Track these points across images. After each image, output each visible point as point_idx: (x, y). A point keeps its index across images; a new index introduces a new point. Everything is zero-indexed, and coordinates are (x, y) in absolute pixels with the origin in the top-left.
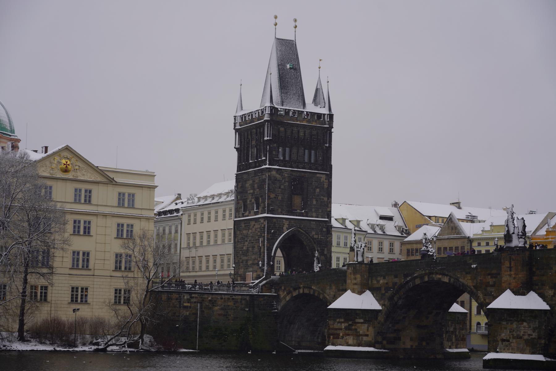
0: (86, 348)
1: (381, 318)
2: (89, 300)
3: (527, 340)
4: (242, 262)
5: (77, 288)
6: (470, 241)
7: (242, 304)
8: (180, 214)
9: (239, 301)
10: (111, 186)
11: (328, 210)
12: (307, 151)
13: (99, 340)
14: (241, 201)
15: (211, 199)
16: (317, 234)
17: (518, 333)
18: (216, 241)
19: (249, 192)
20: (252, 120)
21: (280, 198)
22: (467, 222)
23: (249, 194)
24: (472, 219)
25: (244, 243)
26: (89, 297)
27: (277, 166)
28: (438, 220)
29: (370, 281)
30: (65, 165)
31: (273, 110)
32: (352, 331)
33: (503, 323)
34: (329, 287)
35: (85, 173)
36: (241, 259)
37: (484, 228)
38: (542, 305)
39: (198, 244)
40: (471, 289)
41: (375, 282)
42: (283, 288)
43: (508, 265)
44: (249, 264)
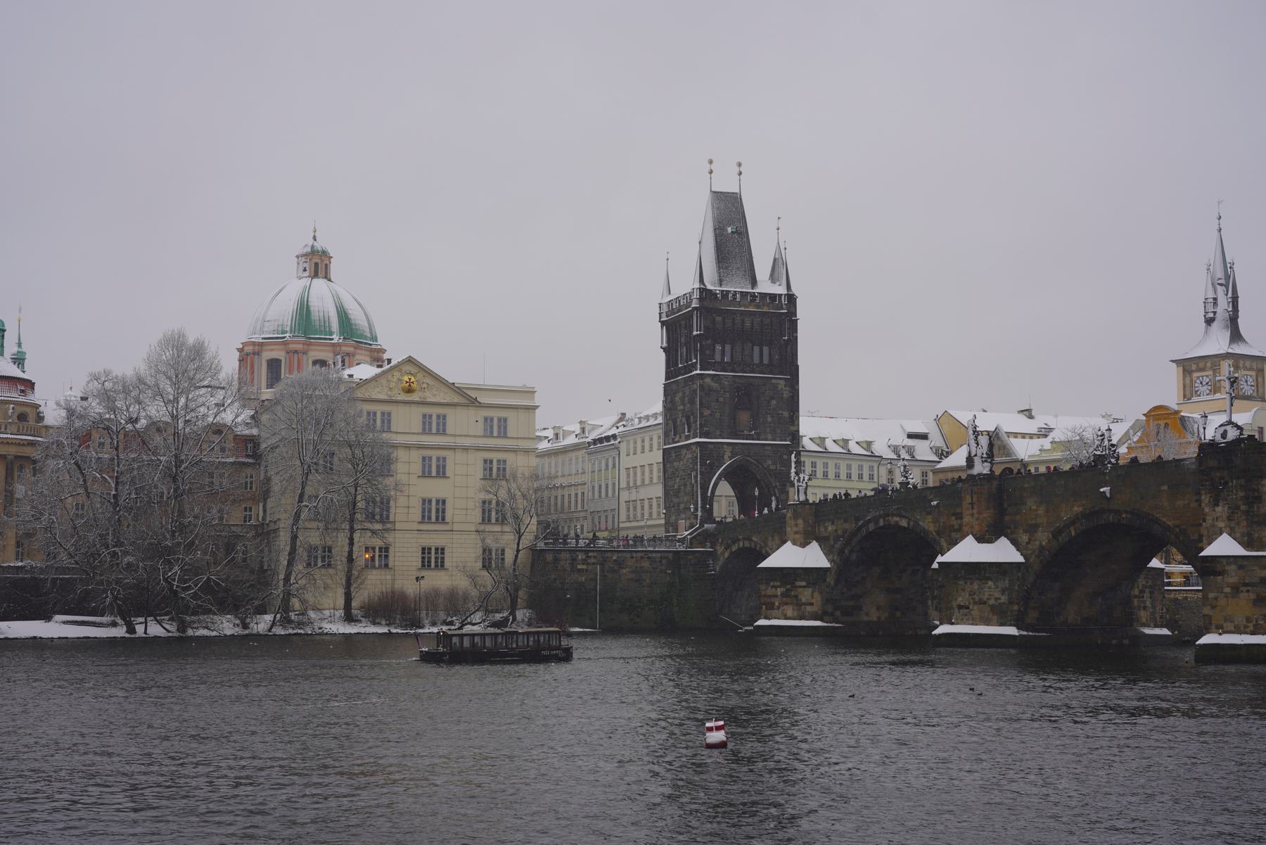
1: (830, 580)
2: (447, 564)
3: (993, 605)
4: (674, 506)
5: (430, 549)
7: (662, 565)
8: (617, 442)
9: (657, 560)
10: (473, 408)
12: (756, 349)
17: (982, 596)
19: (679, 408)
21: (717, 415)
22: (1039, 438)
30: (408, 384)
31: (705, 294)
32: (791, 598)
33: (960, 583)
38: (1016, 557)
41: (822, 529)
42: (720, 541)
43: (970, 502)
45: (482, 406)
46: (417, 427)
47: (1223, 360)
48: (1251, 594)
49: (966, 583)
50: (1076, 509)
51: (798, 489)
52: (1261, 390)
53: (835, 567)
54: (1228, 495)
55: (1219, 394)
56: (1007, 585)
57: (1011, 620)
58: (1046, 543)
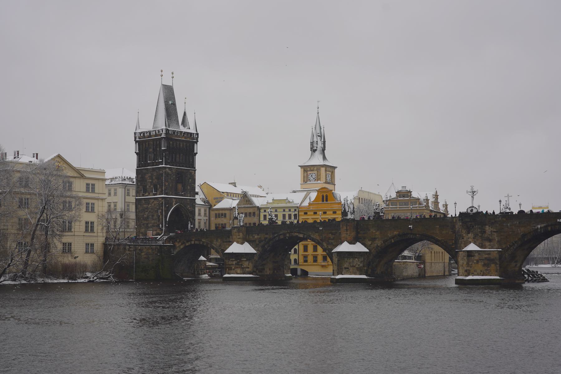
1: (256, 258)
4: (143, 225)
6: (259, 209)
7: (156, 251)
14: (141, 187)
16: (190, 207)
17: (353, 264)
19: (148, 181)
20: (150, 136)
21: (171, 185)
23: (148, 182)
26: (72, 249)
27: (169, 165)
29: (247, 237)
32: (239, 265)
33: (346, 259)
34: (215, 240)
35: (68, 171)
36: (142, 222)
37: (268, 201)
38: (364, 249)
43: (346, 229)
44: (149, 226)
46: (84, 189)
47: (322, 167)
48: (482, 263)
49: (348, 259)
51: (240, 221)
53: (259, 252)
54: (474, 231)
55: (320, 181)
56: (363, 260)
58: (380, 245)
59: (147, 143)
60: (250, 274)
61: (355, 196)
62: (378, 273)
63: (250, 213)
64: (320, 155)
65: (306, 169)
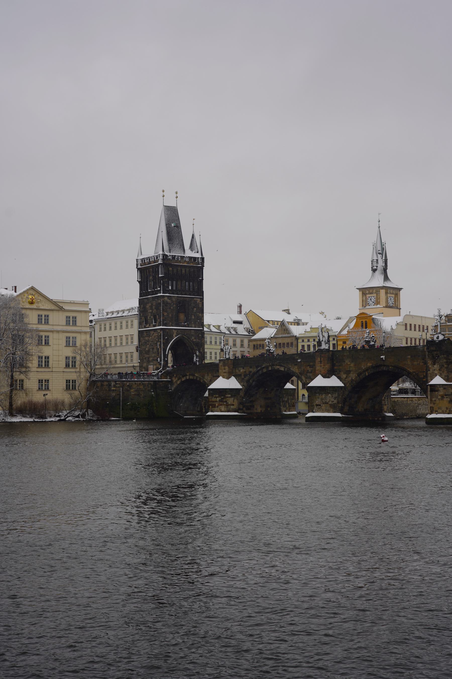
0: (53, 419)
1: (242, 394)
2: (50, 388)
4: (145, 359)
6: (297, 338)
9: (146, 385)
11: (202, 322)
12: (187, 283)
13: (60, 414)
15: (116, 313)
16: (195, 338)
17: (326, 400)
18: (121, 343)
19: (149, 311)
20: (150, 263)
21: (170, 315)
24: (297, 323)
25: (146, 346)
28: (274, 322)
33: (317, 395)
34: (207, 375)
38: (339, 383)
39: (108, 345)
40: (298, 375)
45: (65, 311)
49: (319, 395)
50: (369, 364)
52: (396, 304)
57: (338, 410)
59: (148, 271)
60: (235, 412)
61: (398, 322)
62: (360, 410)
63: (288, 344)
64: (381, 275)
65: (364, 291)
